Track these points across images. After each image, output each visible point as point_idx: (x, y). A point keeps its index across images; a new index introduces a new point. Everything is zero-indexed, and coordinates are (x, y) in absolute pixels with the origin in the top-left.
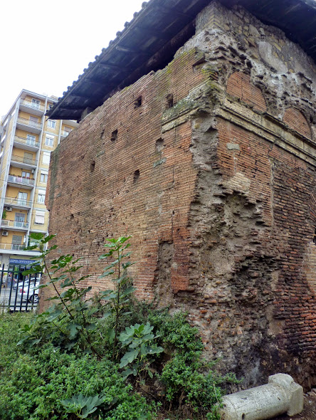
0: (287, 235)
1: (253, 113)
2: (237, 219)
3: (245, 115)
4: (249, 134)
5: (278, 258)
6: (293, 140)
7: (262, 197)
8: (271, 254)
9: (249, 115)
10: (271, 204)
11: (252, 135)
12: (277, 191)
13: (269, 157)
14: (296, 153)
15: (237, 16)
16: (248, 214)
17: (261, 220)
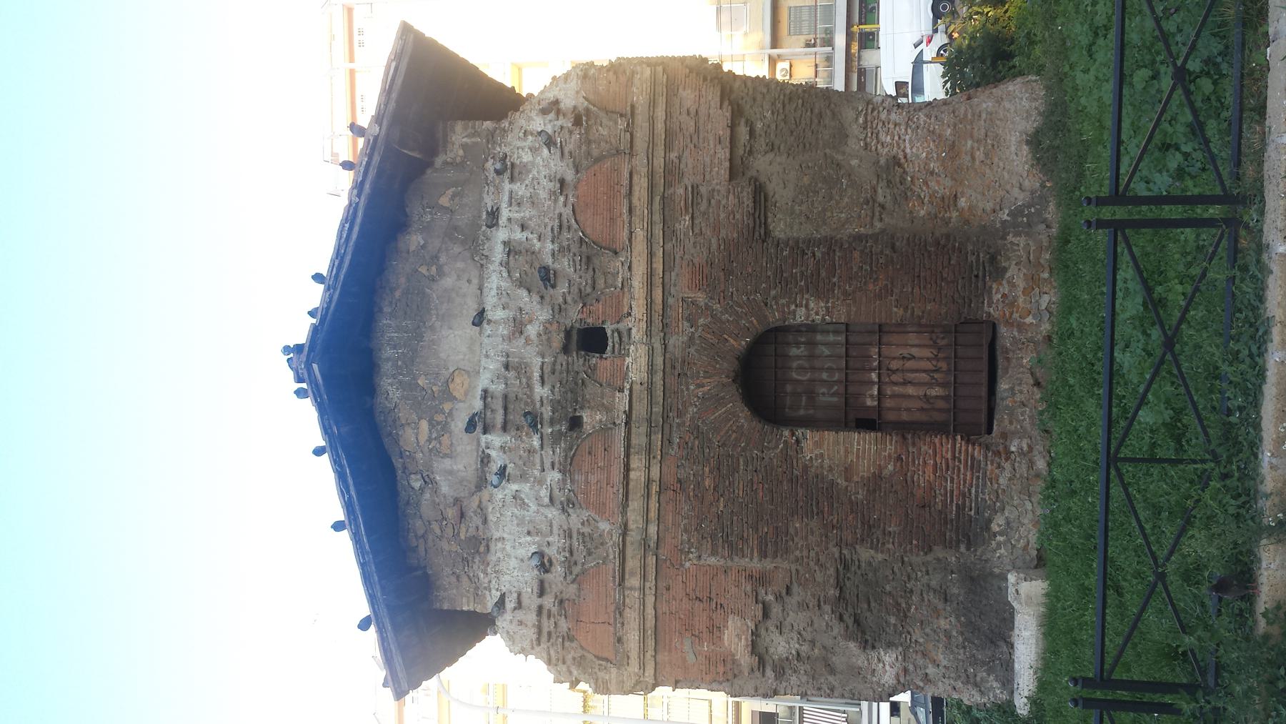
0: (798, 525)
1: (627, 610)
2: (787, 623)
3: (636, 627)
4: (660, 612)
5: (836, 550)
6: (635, 504)
7: (749, 588)
8: (832, 571)
9: (631, 616)
10: (756, 564)
11: (659, 606)
12: (734, 550)
13: (682, 565)
14: (655, 488)
15: (426, 550)
16: (776, 610)
17: (784, 592)
